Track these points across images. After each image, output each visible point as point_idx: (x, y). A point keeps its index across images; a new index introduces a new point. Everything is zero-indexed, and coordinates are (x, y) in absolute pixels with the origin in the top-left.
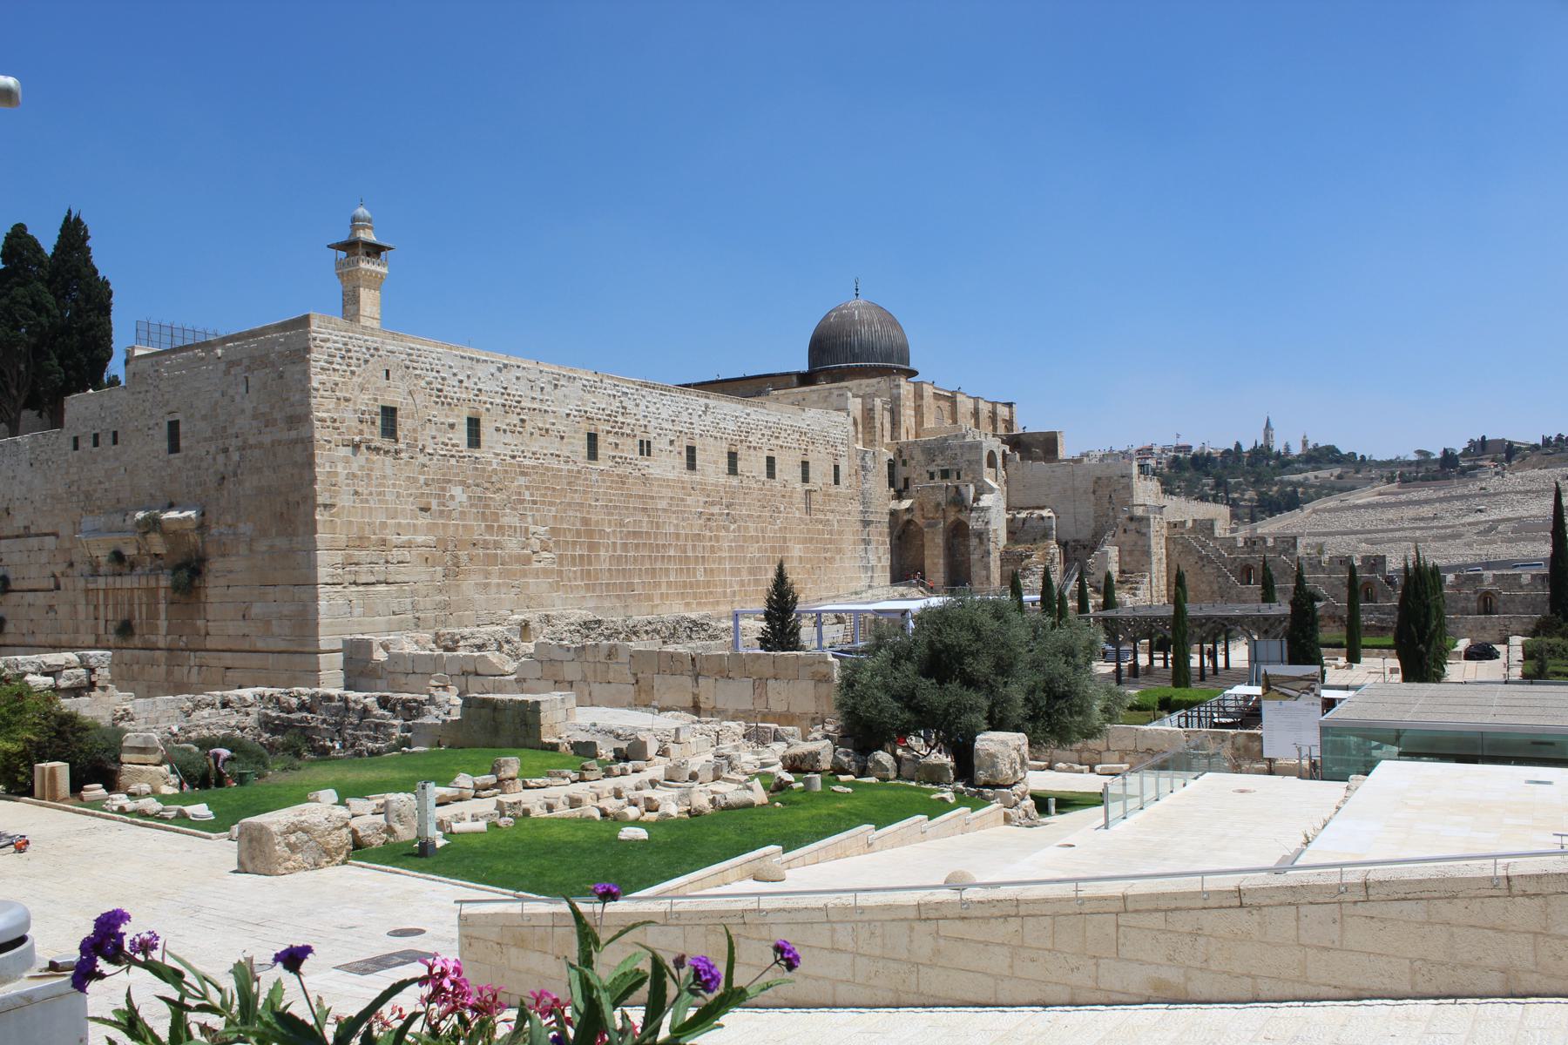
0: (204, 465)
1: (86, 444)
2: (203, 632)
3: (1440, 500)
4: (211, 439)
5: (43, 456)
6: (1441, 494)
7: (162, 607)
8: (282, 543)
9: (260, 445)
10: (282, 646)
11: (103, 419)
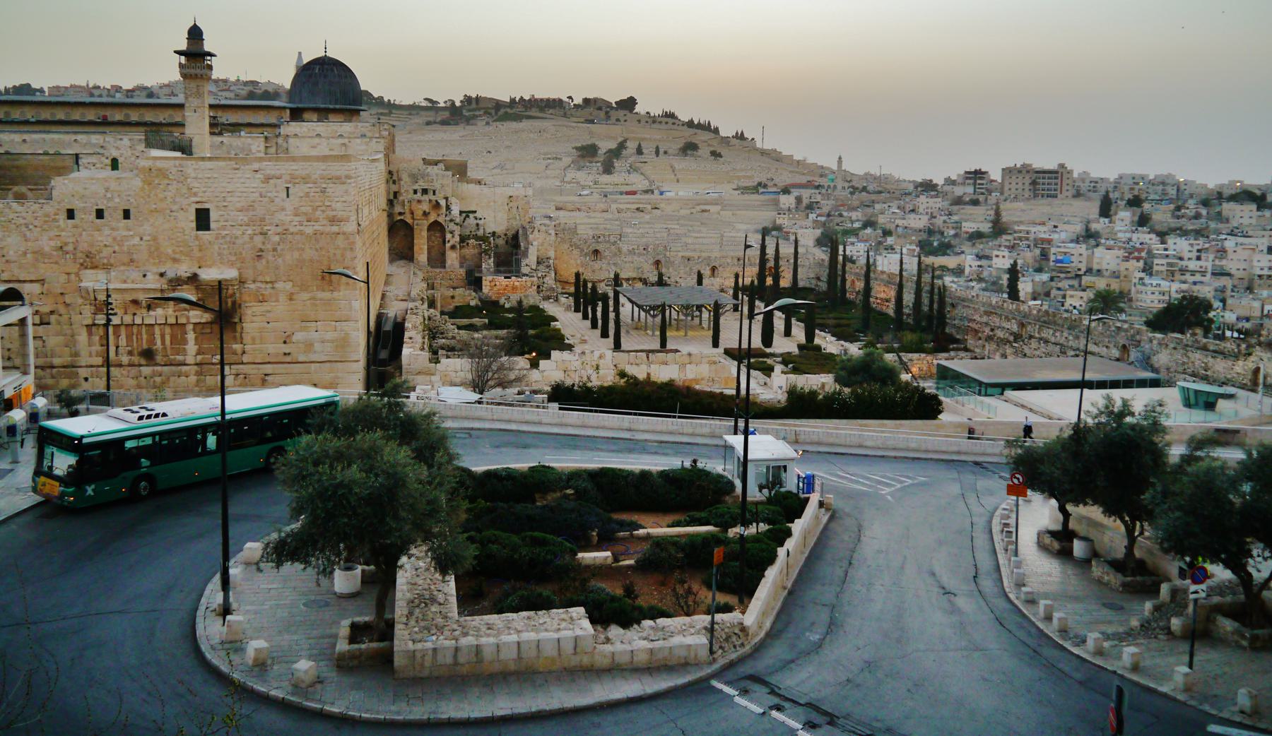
0: (239, 241)
1: (86, 217)
4: (248, 225)
5: (22, 221)
6: (456, 136)
8: (327, 295)
9: (301, 233)
11: (111, 199)
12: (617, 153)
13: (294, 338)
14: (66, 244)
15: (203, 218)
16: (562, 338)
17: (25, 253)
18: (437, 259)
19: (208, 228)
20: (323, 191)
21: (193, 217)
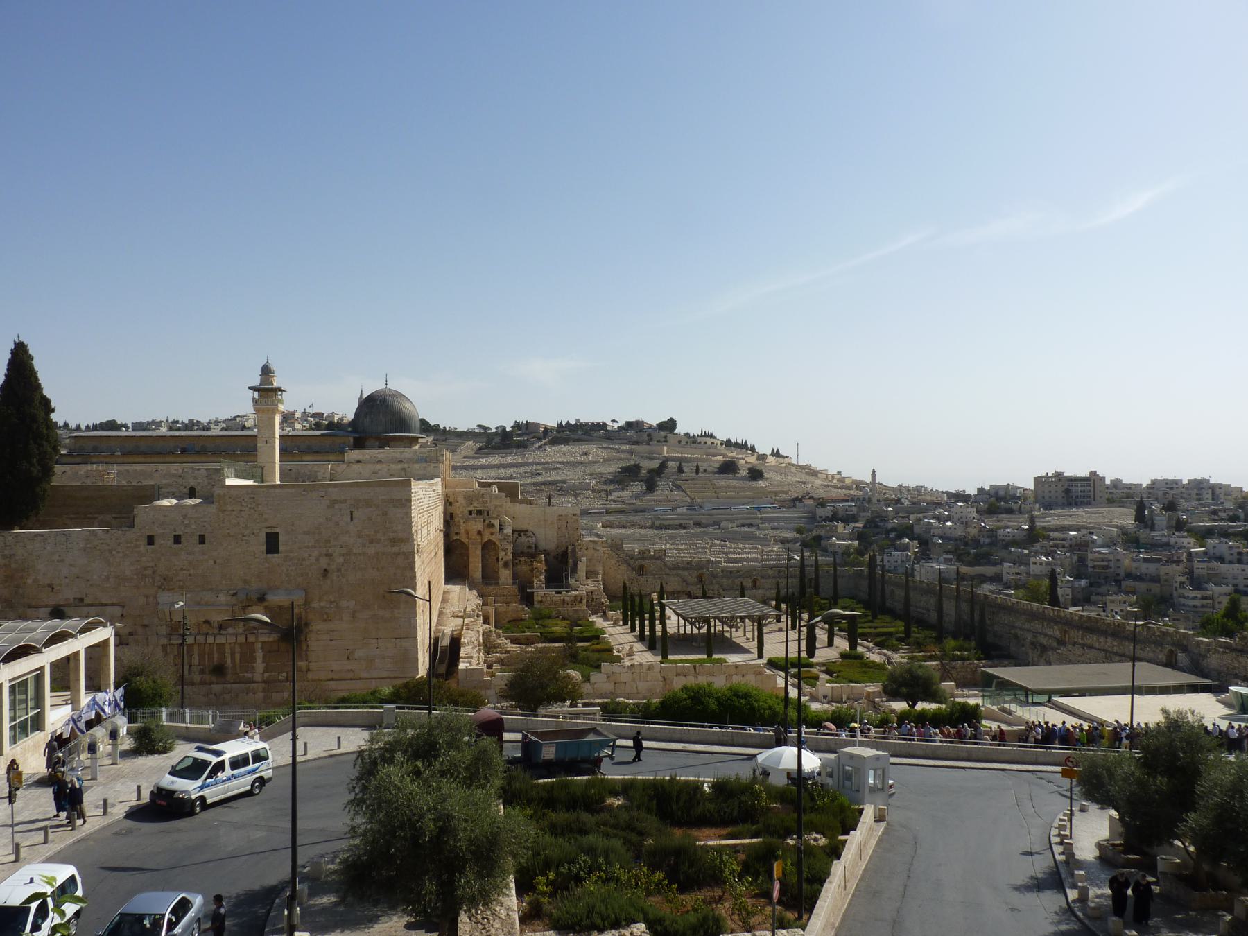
2: (305, 669)
3: (511, 466)
6: (509, 459)
7: (259, 655)
10: (385, 674)
12: (659, 471)
13: (357, 655)
14: (146, 568)
15: (272, 543)
16: (610, 650)
17: (108, 578)
18: (489, 578)
19: (277, 551)
20: (385, 514)
21: (263, 538)
